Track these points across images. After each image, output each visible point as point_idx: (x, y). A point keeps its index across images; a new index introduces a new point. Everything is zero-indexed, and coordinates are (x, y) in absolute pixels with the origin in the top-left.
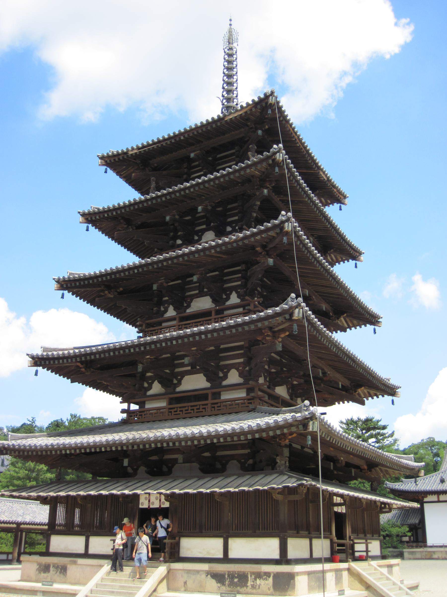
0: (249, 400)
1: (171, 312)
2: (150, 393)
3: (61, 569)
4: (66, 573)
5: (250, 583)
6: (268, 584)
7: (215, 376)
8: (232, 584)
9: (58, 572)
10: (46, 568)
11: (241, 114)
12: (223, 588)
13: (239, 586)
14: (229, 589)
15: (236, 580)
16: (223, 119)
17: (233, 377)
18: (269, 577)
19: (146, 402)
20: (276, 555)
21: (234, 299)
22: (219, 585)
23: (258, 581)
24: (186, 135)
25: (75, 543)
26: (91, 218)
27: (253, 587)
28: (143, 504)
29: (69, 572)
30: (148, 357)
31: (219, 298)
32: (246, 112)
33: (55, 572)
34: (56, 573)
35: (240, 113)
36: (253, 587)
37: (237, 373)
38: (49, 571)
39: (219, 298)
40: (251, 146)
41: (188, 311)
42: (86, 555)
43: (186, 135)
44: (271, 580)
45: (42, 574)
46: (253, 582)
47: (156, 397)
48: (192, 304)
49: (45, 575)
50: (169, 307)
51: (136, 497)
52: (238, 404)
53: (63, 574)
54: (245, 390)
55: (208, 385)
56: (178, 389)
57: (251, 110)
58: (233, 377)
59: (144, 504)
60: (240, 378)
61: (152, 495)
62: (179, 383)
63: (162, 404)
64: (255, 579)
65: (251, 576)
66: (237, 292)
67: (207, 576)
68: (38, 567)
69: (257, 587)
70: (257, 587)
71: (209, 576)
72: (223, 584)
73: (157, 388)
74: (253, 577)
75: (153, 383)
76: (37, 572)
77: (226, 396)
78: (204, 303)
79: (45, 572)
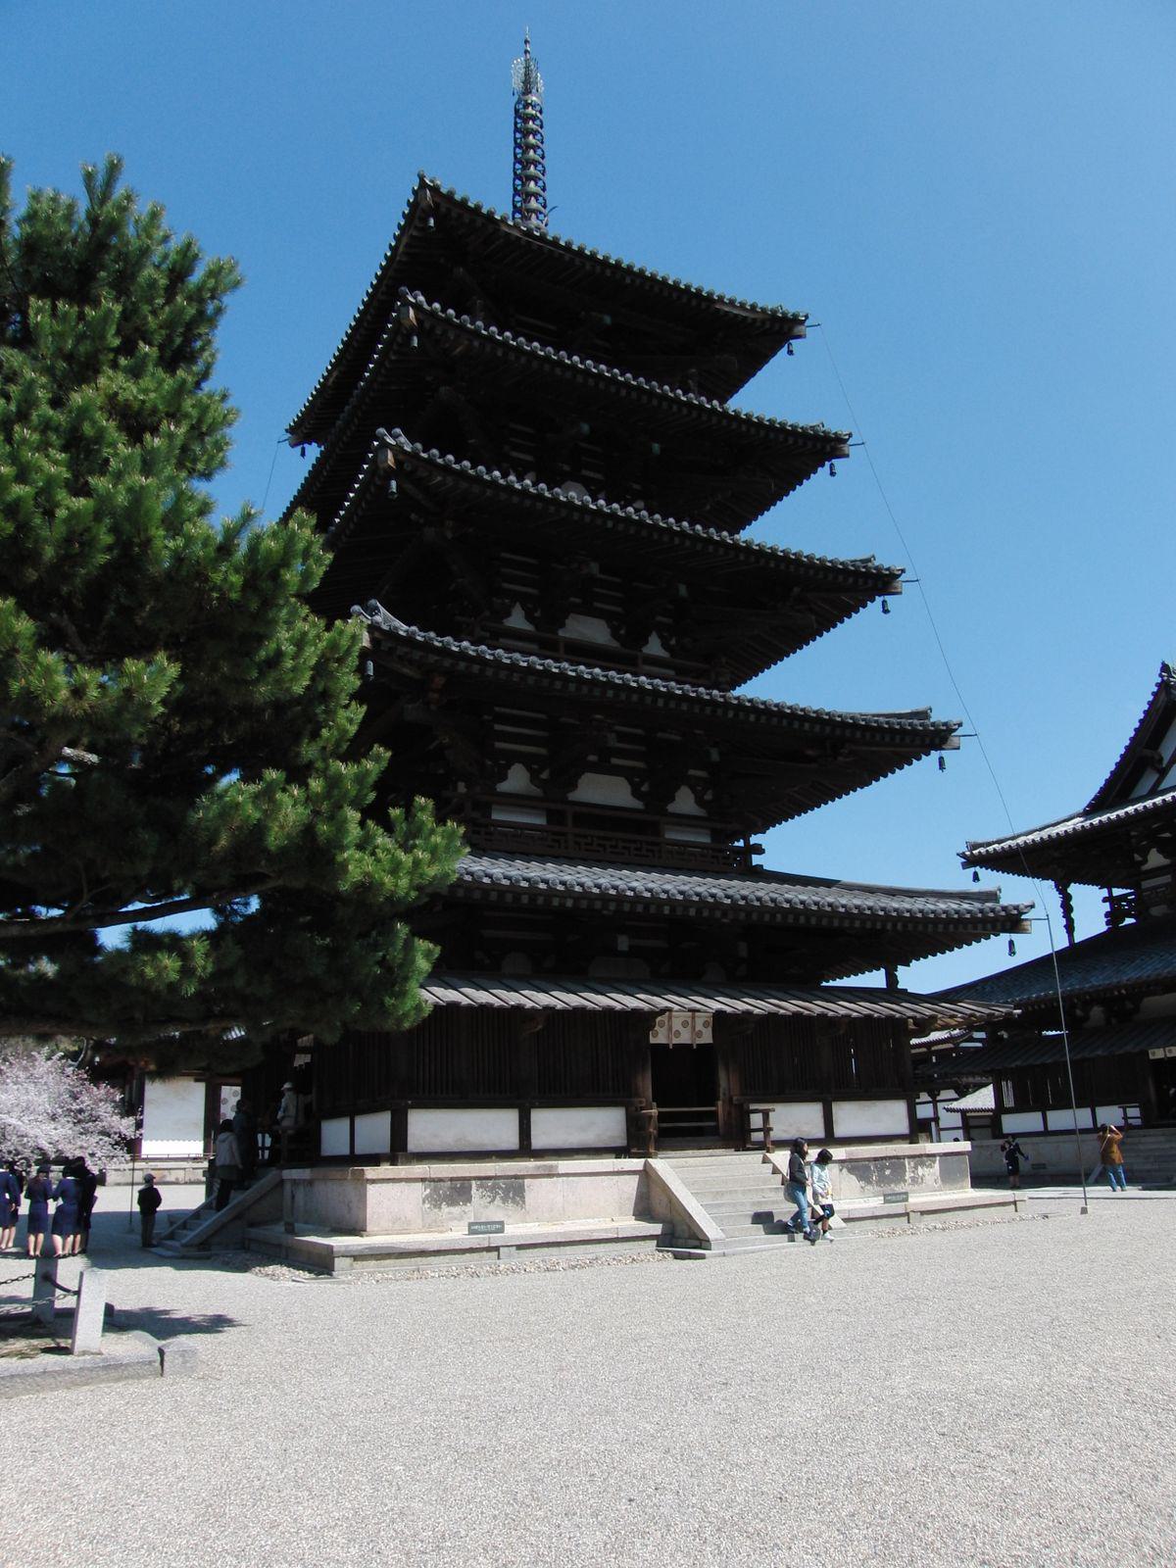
0: (713, 850)
1: (517, 620)
2: (504, 787)
3: (506, 1191)
4: (523, 1198)
5: (908, 1175)
6: (934, 1174)
7: (656, 791)
8: (883, 1180)
9: (498, 1200)
10: (459, 1191)
11: (746, 317)
12: (869, 1187)
13: (892, 1181)
14: (879, 1188)
15: (888, 1172)
16: (714, 301)
17: (685, 802)
18: (934, 1162)
19: (494, 807)
20: (903, 1127)
21: (654, 647)
22: (862, 1183)
23: (920, 1171)
24: (638, 281)
25: (497, 1126)
26: (433, 328)
27: (914, 1180)
28: (656, 1035)
29: (527, 1194)
30: (598, 717)
31: (631, 634)
32: (754, 320)
33: (489, 1200)
34: (495, 1198)
35: (744, 314)
36: (914, 1180)
37: (692, 796)
38: (469, 1200)
39: (631, 634)
40: (694, 370)
41: (561, 633)
42: (525, 1149)
43: (638, 281)
44: (937, 1165)
45: (445, 1209)
46: (913, 1172)
47: (515, 801)
48: (567, 621)
49: (456, 1210)
50: (513, 607)
51: (644, 1020)
52: (693, 854)
53: (514, 1202)
54: (709, 832)
55: (638, 804)
56: (574, 796)
57: (763, 322)
58: (685, 802)
59: (659, 1037)
60: (695, 805)
61: (684, 1016)
62: (573, 785)
63: (540, 820)
64: (916, 1168)
65: (909, 1164)
66: (661, 637)
67: (841, 1170)
68: (428, 1191)
69: (920, 1180)
70: (920, 1180)
71: (845, 1170)
72: (869, 1181)
73: (517, 780)
74: (912, 1164)
75: (509, 768)
76: (427, 1206)
77: (672, 835)
78: (592, 630)
79: (452, 1203)
